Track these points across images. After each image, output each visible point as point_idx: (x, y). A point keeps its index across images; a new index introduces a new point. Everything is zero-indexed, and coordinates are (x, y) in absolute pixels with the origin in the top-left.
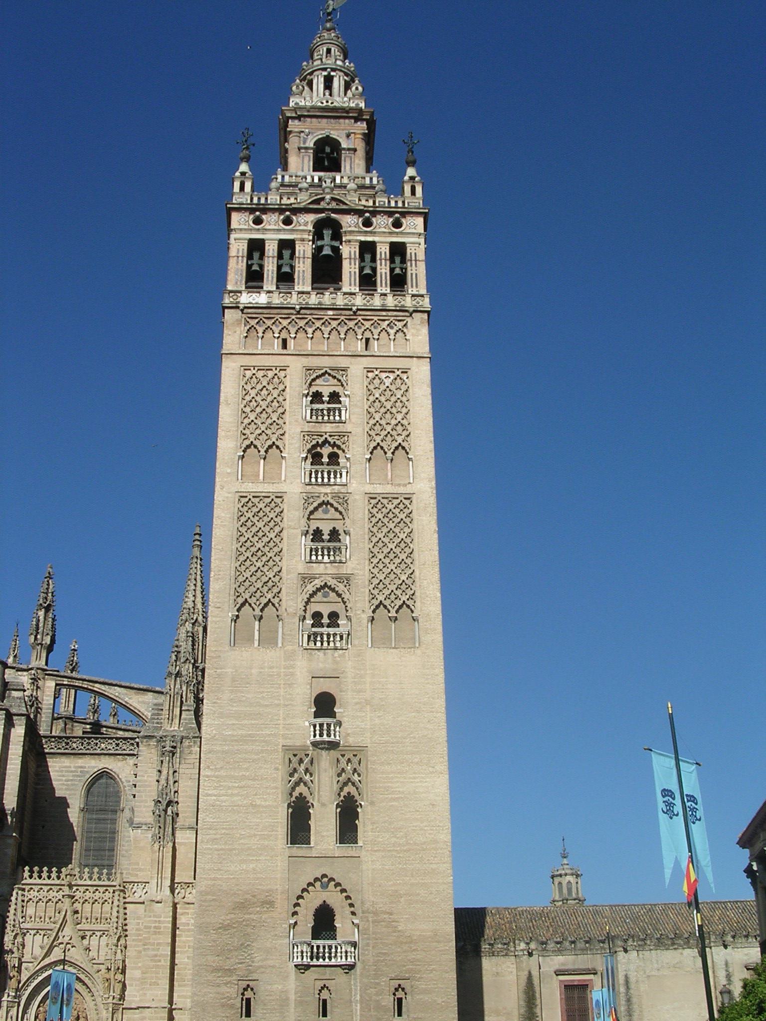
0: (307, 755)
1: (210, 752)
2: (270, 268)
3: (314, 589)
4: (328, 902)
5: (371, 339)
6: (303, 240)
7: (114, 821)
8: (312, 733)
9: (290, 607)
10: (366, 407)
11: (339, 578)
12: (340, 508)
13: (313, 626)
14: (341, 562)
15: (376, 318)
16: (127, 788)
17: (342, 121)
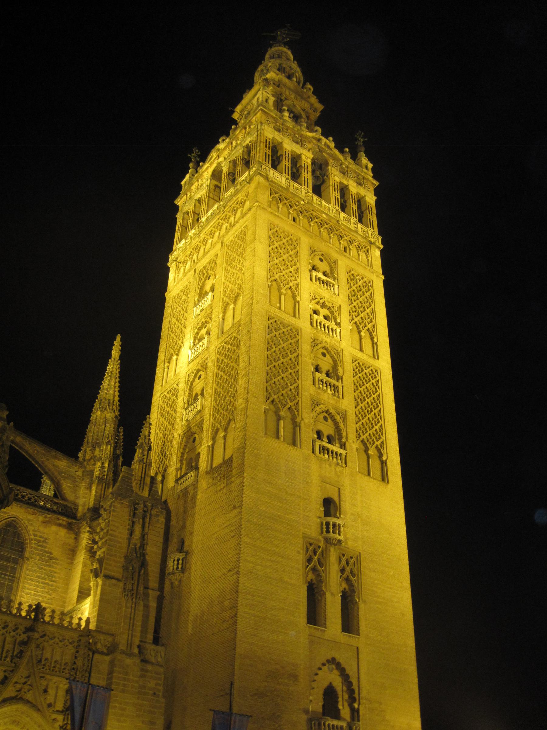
0: (319, 547)
1: (248, 521)
2: (287, 164)
3: (321, 411)
4: (335, 684)
5: (348, 248)
6: (307, 158)
7: (14, 570)
8: (325, 530)
9: (306, 418)
10: (348, 292)
11: (336, 409)
12: (335, 357)
13: (317, 438)
14: (338, 397)
15: (351, 236)
16: (33, 542)
17: (303, 102)
